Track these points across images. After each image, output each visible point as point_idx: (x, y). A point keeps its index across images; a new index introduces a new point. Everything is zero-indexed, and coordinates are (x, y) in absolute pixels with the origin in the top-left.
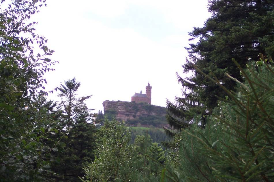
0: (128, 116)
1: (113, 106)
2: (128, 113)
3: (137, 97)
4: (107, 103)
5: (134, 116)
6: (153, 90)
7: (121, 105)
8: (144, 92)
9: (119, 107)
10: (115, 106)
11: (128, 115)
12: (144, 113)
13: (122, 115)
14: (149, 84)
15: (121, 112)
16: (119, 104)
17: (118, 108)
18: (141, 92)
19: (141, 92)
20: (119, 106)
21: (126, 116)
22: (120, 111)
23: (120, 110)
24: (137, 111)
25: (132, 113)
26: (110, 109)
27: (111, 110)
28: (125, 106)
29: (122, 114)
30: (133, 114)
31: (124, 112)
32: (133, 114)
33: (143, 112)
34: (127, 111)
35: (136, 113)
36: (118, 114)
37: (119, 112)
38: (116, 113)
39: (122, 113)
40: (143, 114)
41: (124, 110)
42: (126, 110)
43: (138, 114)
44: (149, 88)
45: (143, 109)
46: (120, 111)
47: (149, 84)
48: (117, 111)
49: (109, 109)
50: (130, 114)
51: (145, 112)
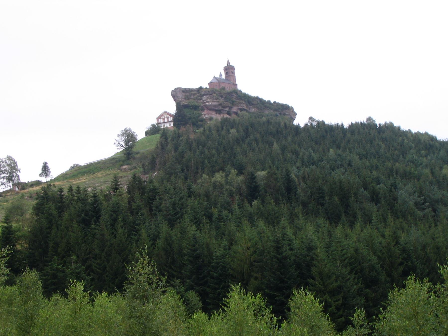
0: (220, 114)
1: (192, 97)
2: (221, 108)
3: (216, 82)
4: (181, 92)
5: (229, 113)
6: (237, 73)
7: (207, 95)
8: (224, 77)
9: (205, 98)
10: (195, 96)
11: (219, 112)
13: (210, 112)
14: (228, 62)
15: (211, 105)
16: (203, 93)
17: (202, 99)
18: (221, 75)
19: (221, 75)
20: (204, 95)
22: (207, 104)
23: (207, 102)
24: (233, 103)
25: (226, 107)
26: (190, 102)
27: (193, 104)
28: (215, 95)
29: (211, 110)
30: (227, 109)
31: (215, 106)
32: (227, 109)
34: (221, 104)
35: (231, 108)
36: (203, 110)
37: (206, 106)
38: (200, 108)
39: (210, 109)
40: (241, 110)
43: (235, 109)
44: (229, 70)
45: (242, 101)
46: (207, 104)
47: (228, 62)
49: (187, 101)
51: (245, 107)
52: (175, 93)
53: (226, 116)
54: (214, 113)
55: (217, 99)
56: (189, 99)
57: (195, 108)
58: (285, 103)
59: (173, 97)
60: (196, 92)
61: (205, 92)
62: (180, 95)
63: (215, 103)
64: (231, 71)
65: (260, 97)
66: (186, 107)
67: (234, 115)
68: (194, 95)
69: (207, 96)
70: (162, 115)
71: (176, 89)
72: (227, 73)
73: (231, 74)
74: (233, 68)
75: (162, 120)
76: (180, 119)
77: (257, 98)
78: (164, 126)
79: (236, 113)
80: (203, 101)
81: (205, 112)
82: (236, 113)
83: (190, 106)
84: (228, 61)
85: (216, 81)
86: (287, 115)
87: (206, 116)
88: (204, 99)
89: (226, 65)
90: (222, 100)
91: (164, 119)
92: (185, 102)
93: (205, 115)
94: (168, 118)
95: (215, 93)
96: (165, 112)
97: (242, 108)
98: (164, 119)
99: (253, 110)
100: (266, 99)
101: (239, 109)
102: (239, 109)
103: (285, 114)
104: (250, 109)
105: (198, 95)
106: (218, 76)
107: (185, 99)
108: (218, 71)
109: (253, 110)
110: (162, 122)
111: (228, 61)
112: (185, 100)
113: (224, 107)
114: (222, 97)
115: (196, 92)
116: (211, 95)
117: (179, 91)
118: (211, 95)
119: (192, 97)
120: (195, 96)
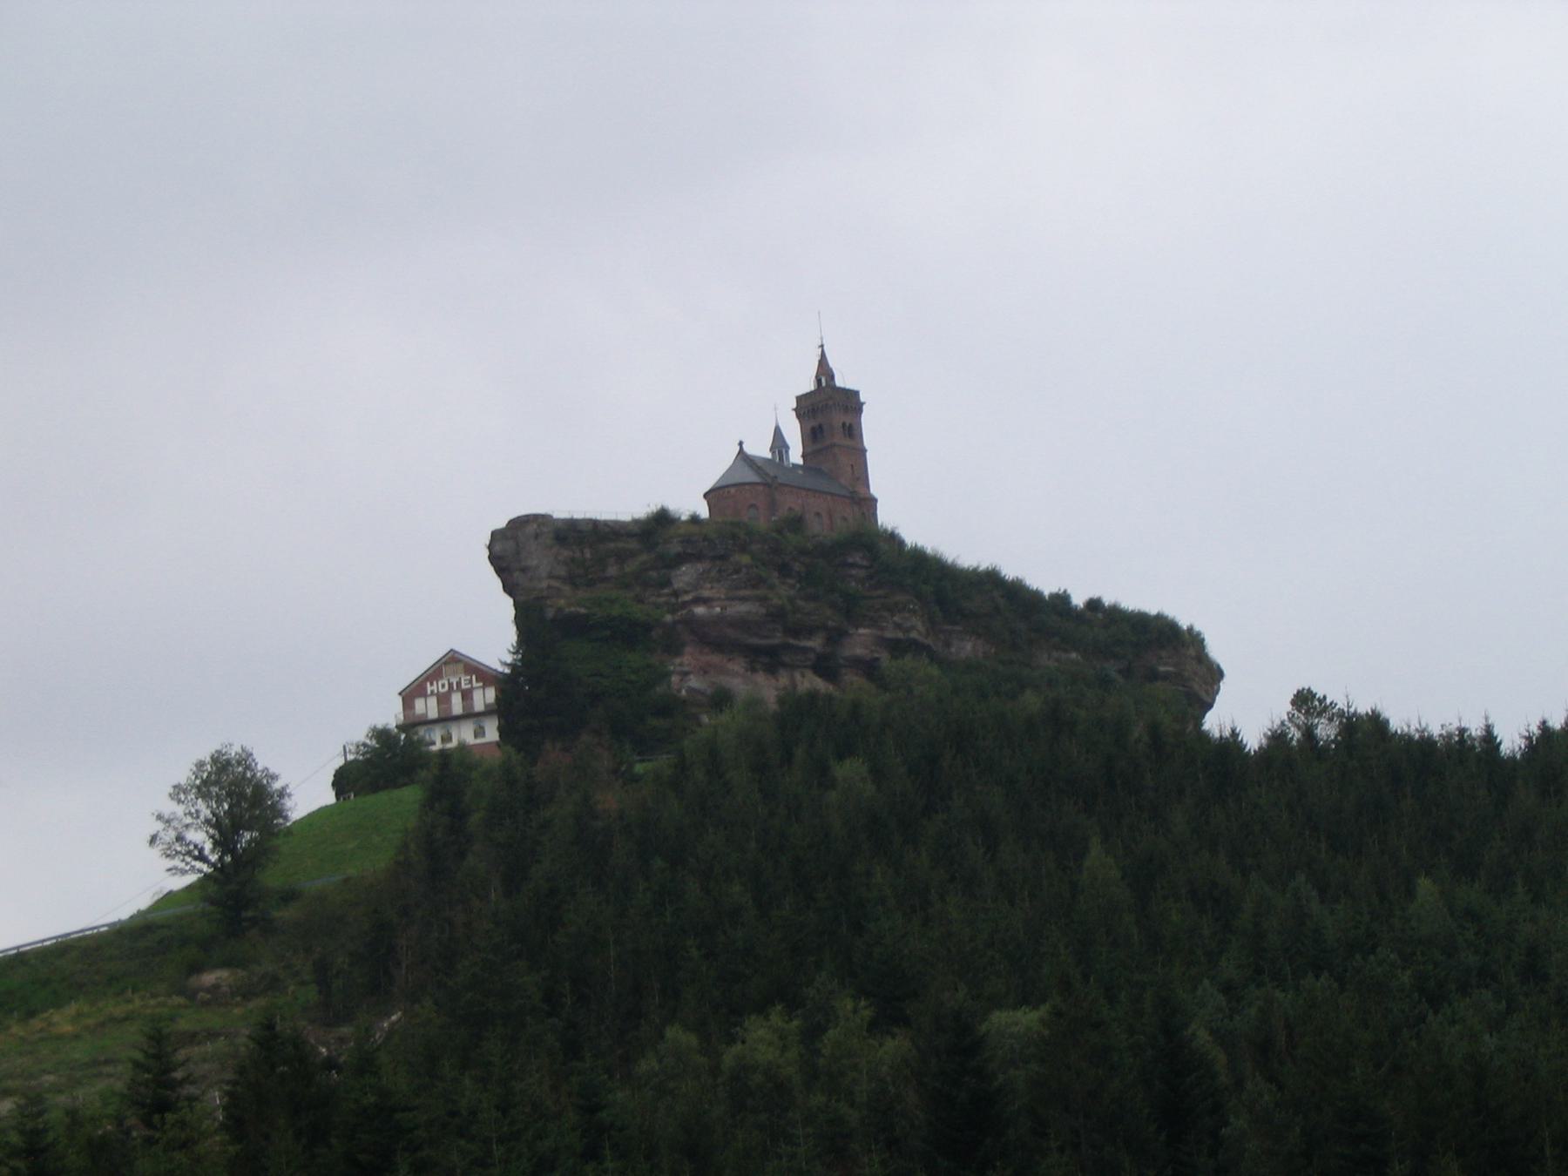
0: (771, 670)
1: (612, 571)
2: (778, 639)
3: (749, 488)
5: (825, 667)
7: (698, 557)
8: (796, 456)
9: (685, 575)
10: (631, 567)
11: (768, 659)
12: (914, 635)
13: (716, 659)
14: (824, 370)
16: (675, 548)
17: (667, 583)
18: (779, 443)
19: (779, 443)
20: (681, 559)
21: (754, 670)
22: (700, 610)
23: (699, 601)
24: (851, 610)
25: (810, 632)
27: (616, 611)
28: (745, 559)
29: (720, 646)
30: (816, 643)
31: (743, 624)
32: (816, 643)
33: (898, 626)
34: (778, 615)
35: (836, 637)
37: (691, 623)
38: (656, 633)
39: (713, 638)
40: (897, 648)
41: (743, 599)
42: (763, 600)
43: (860, 643)
44: (830, 412)
45: (900, 598)
46: (700, 610)
47: (824, 370)
48: (668, 618)
50: (791, 641)
51: (917, 628)
53: (809, 682)
54: (738, 665)
55: (757, 582)
56: (591, 584)
57: (631, 633)
58: (1152, 610)
59: (500, 571)
60: (633, 545)
61: (687, 540)
63: (741, 608)
64: (838, 419)
65: (1009, 572)
66: (574, 626)
67: (854, 680)
68: (622, 557)
69: (700, 567)
70: (434, 673)
71: (518, 524)
72: (813, 435)
73: (840, 439)
74: (850, 402)
75: (433, 702)
76: (533, 694)
77: (992, 579)
78: (447, 738)
79: (869, 668)
80: (676, 594)
81: (688, 659)
82: (869, 668)
84: (823, 362)
85: (752, 477)
86: (1166, 677)
87: (694, 682)
88: (678, 584)
89: (808, 385)
90: (783, 592)
91: (444, 699)
92: (568, 602)
93: (689, 675)
94: (467, 696)
95: (743, 549)
96: (453, 660)
97: (900, 635)
98: (444, 699)
99: (966, 648)
100: (1044, 582)
101: (883, 642)
102: (883, 642)
103: (1153, 676)
104: (948, 645)
105: (644, 557)
106: (761, 449)
107: (571, 580)
108: (765, 420)
109: (966, 648)
110: (433, 713)
111: (823, 362)
112: (567, 589)
113: (797, 631)
114: (784, 570)
115: (633, 545)
116: (723, 558)
117: (537, 536)
118: (723, 558)
119: (612, 571)
120: (631, 567)
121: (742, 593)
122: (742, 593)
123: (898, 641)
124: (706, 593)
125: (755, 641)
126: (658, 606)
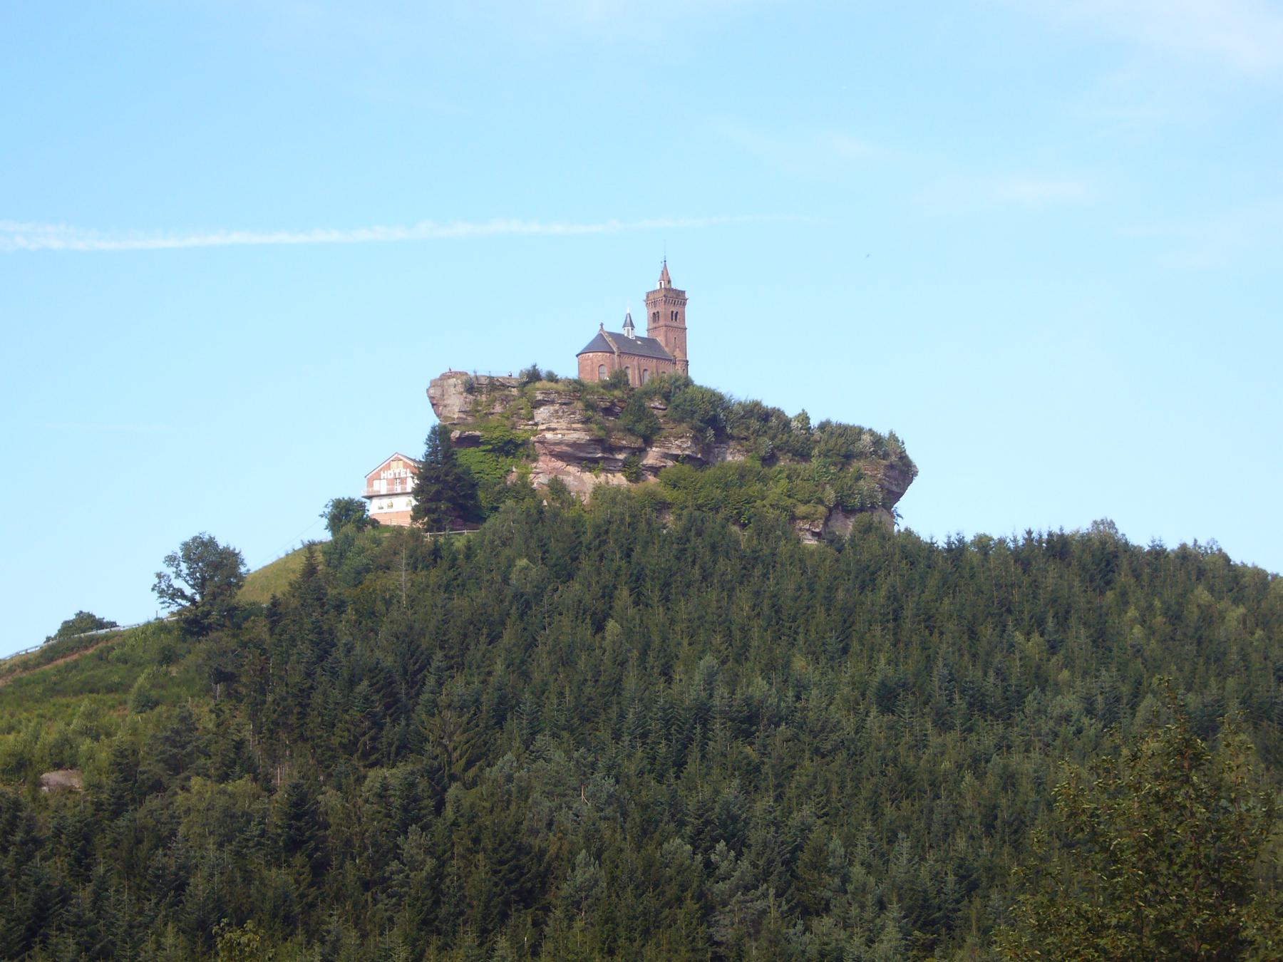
7: (552, 402)
9: (542, 413)
15: (560, 443)
17: (532, 418)
18: (630, 324)
22: (549, 435)
23: (549, 429)
25: (621, 449)
31: (574, 445)
37: (542, 442)
43: (652, 457)
44: (670, 304)
46: (549, 435)
52: (439, 392)
53: (619, 480)
62: (456, 403)
63: (573, 436)
79: (655, 470)
80: (536, 424)
83: (488, 443)
84: (665, 272)
93: (540, 474)
97: (679, 452)
98: (391, 482)
101: (666, 456)
111: (665, 272)
121: (575, 426)
122: (575, 426)
123: (678, 456)
124: (553, 425)
125: (582, 455)
126: (526, 431)
